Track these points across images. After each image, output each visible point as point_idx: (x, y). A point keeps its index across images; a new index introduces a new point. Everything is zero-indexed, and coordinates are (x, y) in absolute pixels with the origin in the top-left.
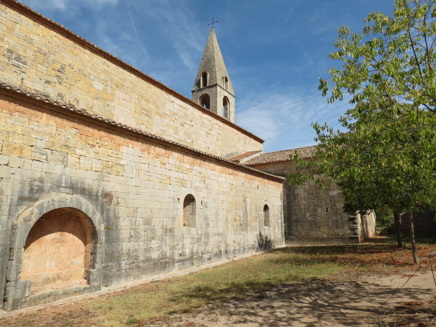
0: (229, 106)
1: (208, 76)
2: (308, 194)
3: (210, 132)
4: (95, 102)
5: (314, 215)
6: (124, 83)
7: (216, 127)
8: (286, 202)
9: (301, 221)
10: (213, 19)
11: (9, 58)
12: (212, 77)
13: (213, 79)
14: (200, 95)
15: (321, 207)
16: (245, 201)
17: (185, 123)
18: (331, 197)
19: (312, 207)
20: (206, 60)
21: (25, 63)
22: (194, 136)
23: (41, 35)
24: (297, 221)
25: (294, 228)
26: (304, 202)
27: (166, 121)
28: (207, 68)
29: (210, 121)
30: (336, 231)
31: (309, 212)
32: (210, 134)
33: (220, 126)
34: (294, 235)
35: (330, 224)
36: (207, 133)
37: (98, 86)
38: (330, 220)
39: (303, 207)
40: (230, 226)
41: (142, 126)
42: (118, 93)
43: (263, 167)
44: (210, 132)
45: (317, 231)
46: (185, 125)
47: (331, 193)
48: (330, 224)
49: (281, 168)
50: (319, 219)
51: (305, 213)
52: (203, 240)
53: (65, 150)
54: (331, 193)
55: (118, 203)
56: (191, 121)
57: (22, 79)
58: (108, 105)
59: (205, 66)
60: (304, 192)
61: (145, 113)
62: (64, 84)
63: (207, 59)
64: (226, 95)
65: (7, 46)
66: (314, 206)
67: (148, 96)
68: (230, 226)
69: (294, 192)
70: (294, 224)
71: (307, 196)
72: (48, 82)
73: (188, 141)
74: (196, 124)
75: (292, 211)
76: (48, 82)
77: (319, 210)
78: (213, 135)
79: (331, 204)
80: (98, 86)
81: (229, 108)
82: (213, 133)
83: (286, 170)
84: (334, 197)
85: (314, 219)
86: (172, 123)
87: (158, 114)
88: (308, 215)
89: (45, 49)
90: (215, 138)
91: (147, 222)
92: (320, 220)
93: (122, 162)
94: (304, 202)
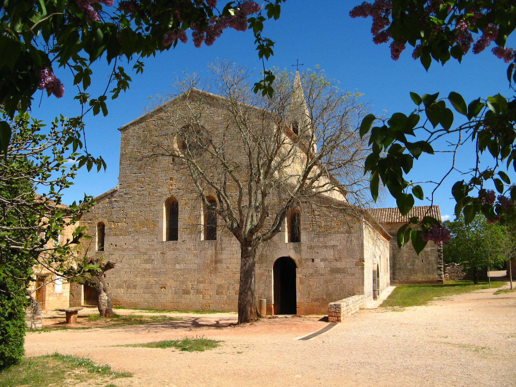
2: (409, 249)
5: (413, 265)
8: (392, 254)
9: (403, 269)
10: (297, 60)
15: (418, 259)
19: (411, 259)
25: (398, 274)
30: (428, 276)
31: (409, 262)
34: (397, 279)
35: (424, 271)
38: (424, 269)
39: (405, 258)
45: (414, 276)
48: (424, 271)
50: (416, 267)
51: (406, 264)
66: (413, 258)
71: (408, 250)
77: (417, 261)
84: (427, 252)
85: (412, 268)
88: (408, 264)
92: (417, 268)
94: (406, 255)
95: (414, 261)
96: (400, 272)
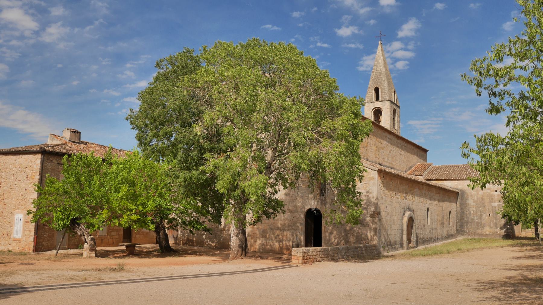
5: (481, 217)
9: (470, 222)
10: (380, 32)
12: (384, 93)
13: (385, 94)
15: (485, 213)
16: (443, 209)
17: (391, 150)
18: (493, 207)
19: (479, 213)
20: (376, 74)
24: (467, 222)
26: (473, 209)
27: (384, 151)
28: (378, 82)
30: (496, 230)
31: (476, 216)
33: (405, 146)
38: (492, 223)
39: (472, 212)
41: (377, 159)
43: (442, 182)
47: (493, 204)
48: (492, 225)
49: (456, 184)
50: (483, 221)
51: (473, 216)
54: (493, 204)
59: (376, 80)
60: (474, 202)
63: (378, 73)
66: (481, 212)
69: (466, 202)
70: (465, 224)
75: (464, 215)
77: (484, 215)
79: (493, 212)
83: (460, 185)
88: (475, 218)
90: (403, 157)
91: (420, 223)
92: (484, 222)
94: (473, 209)
95: (481, 215)
96: (467, 225)
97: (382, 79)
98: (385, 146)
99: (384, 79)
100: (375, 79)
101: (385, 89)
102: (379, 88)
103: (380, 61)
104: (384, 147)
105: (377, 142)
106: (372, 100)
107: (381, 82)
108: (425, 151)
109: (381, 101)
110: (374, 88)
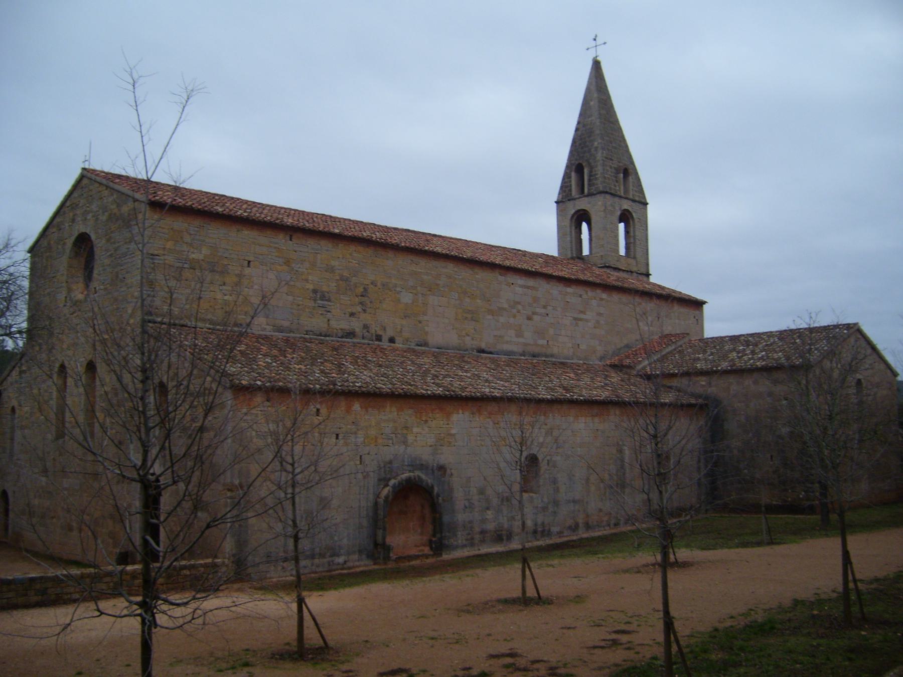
0: (634, 228)
1: (586, 171)
3: (582, 316)
4: (404, 322)
6: (439, 282)
7: (594, 303)
11: (315, 300)
14: (573, 211)
17: (534, 313)
21: (329, 300)
22: (551, 331)
23: (341, 256)
27: (502, 320)
29: (581, 296)
32: (580, 320)
33: (602, 299)
36: (575, 319)
37: (406, 298)
40: (593, 488)
41: (468, 338)
42: (433, 300)
44: (582, 316)
46: (535, 317)
52: (551, 509)
53: (405, 432)
55: (452, 474)
56: (545, 307)
57: (329, 320)
58: (420, 322)
59: (582, 148)
61: (469, 316)
62: (369, 310)
64: (625, 207)
65: (311, 287)
67: (474, 289)
68: (593, 488)
72: (352, 314)
73: (541, 342)
74: (553, 309)
76: (352, 314)
78: (587, 321)
80: (406, 298)
81: (634, 231)
82: (589, 315)
86: (512, 320)
87: (491, 312)
89: (346, 274)
91: (482, 492)
93: (453, 431)
97: (593, 144)
98: (506, 306)
99: (596, 144)
100: (580, 144)
101: (596, 167)
102: (584, 164)
103: (592, 103)
104: (501, 309)
105: (467, 300)
106: (571, 194)
107: (589, 151)
108: (698, 304)
109: (587, 196)
110: (574, 167)
